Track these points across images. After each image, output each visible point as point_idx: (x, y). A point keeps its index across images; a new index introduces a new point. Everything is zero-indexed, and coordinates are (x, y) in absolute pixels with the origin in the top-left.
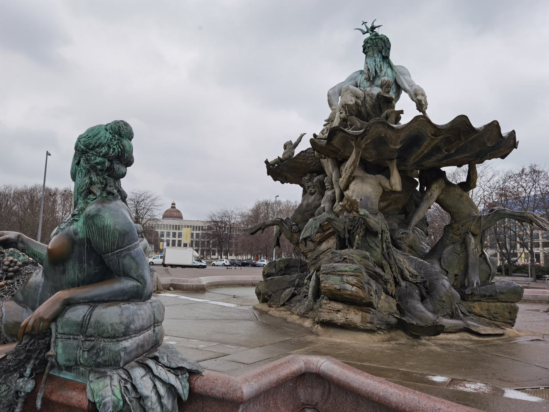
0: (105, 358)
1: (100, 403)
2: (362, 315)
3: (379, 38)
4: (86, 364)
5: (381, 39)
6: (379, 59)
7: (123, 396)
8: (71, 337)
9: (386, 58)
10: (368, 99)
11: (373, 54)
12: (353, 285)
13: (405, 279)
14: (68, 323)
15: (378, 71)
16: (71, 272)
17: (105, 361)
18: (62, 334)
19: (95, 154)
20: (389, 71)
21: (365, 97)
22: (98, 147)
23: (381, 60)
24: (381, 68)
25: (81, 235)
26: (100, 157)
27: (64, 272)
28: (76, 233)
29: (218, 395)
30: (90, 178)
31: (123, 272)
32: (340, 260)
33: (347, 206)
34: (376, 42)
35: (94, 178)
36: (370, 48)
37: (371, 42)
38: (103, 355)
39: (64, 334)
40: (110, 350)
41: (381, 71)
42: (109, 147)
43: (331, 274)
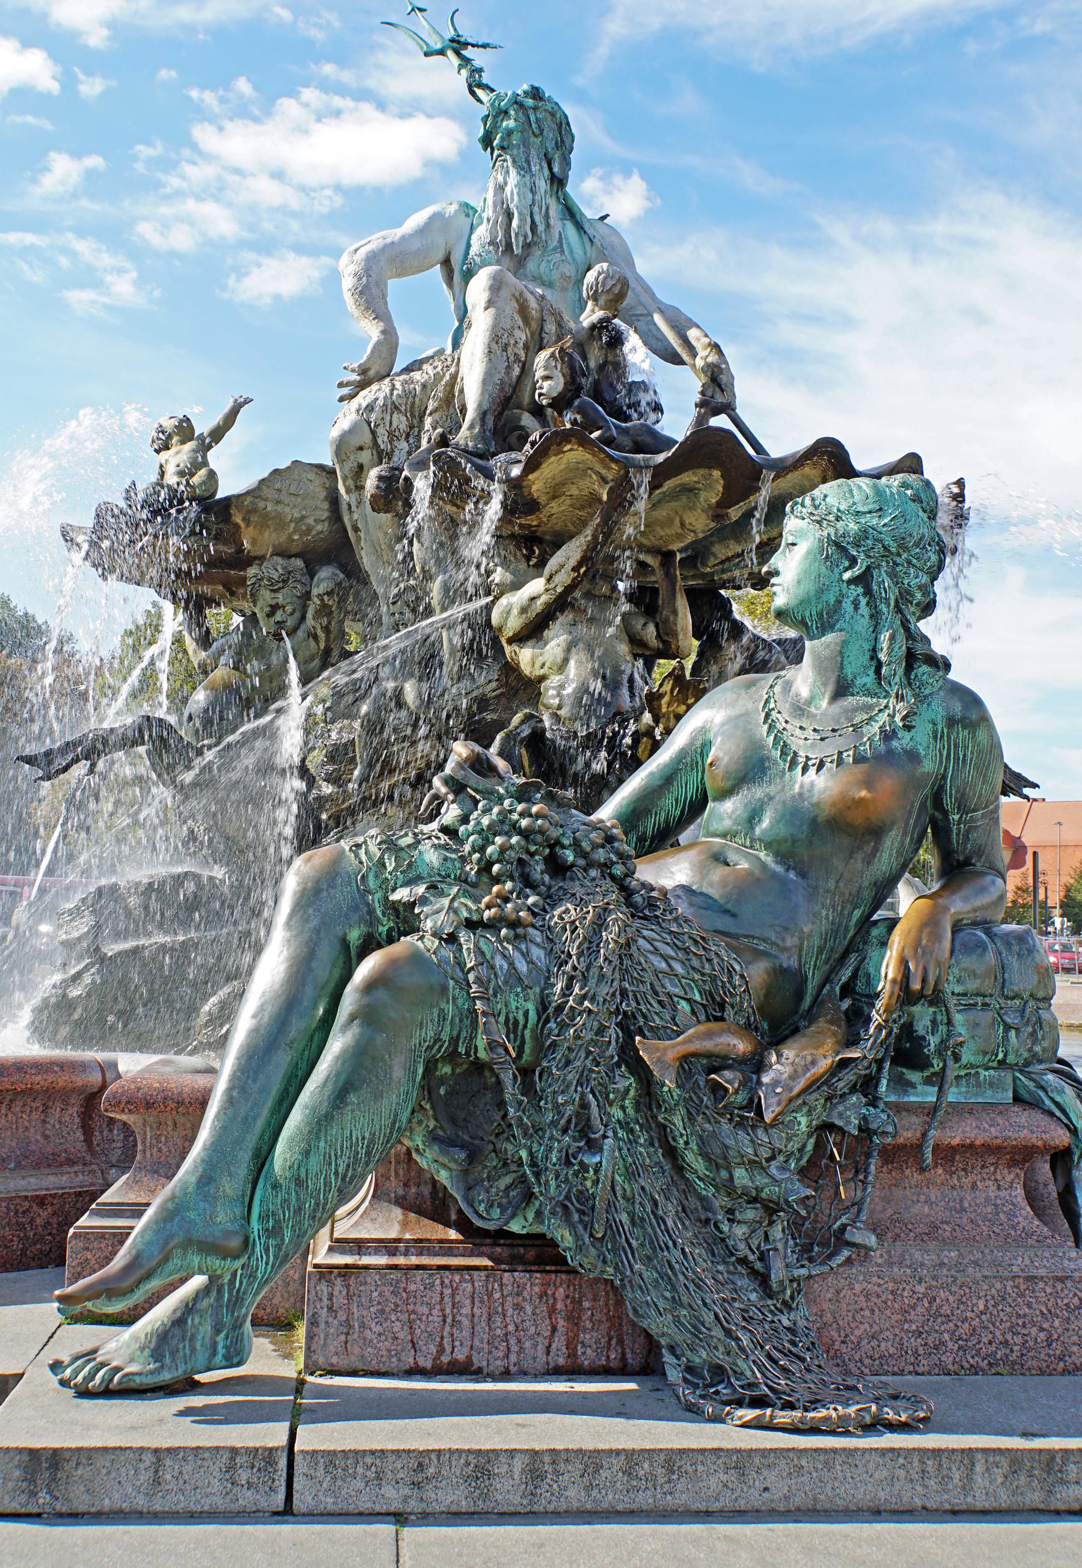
8: (979, 1000)
15: (541, 228)
16: (885, 856)
20: (571, 231)
24: (547, 216)
31: (988, 856)
41: (548, 226)
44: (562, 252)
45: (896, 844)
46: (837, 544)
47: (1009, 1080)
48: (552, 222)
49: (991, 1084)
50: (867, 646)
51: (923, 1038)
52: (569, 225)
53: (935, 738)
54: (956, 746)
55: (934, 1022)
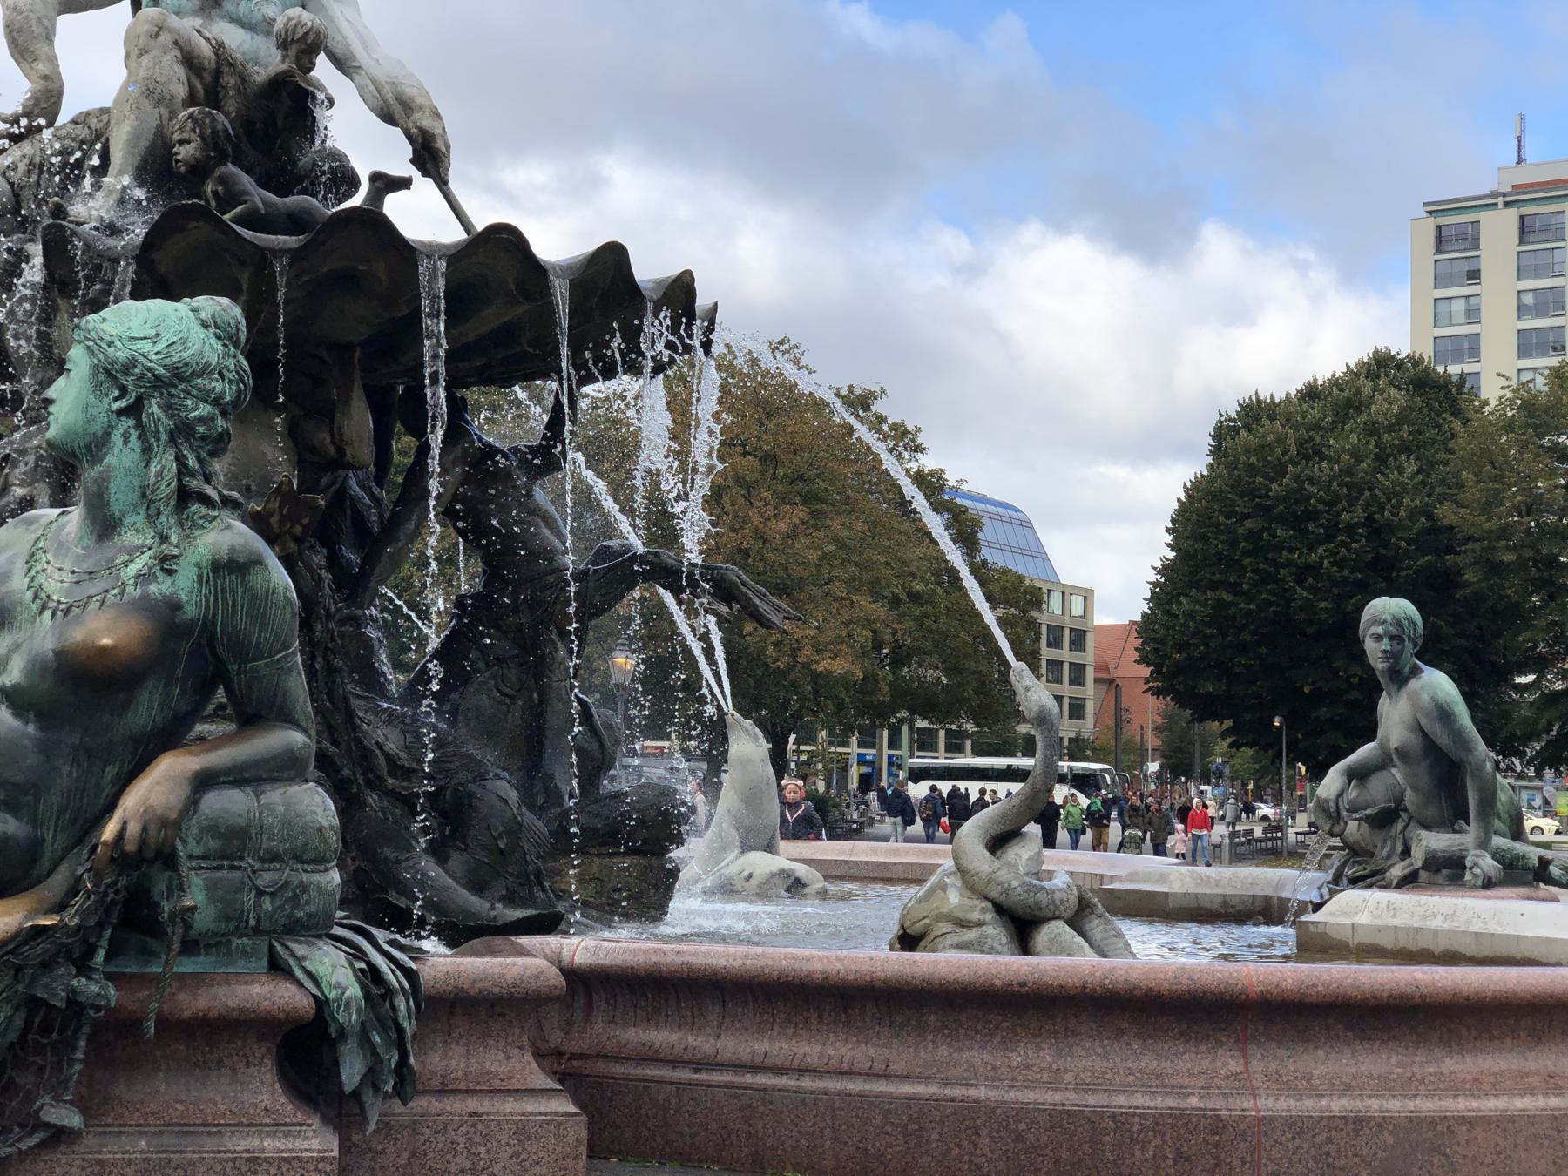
0: (312, 908)
1: (338, 1000)
4: (264, 925)
7: (363, 986)
10: (230, 80)
13: (375, 783)
14: (213, 829)
16: (143, 709)
17: (310, 916)
18: (198, 857)
19: (195, 392)
21: (218, 73)
22: (201, 374)
25: (190, 612)
26: (205, 401)
27: (126, 706)
28: (176, 606)
29: (496, 990)
30: (180, 459)
33: (274, 520)
35: (192, 462)
38: (308, 903)
39: (204, 858)
40: (319, 889)
42: (221, 374)
45: (157, 696)
46: (107, 371)
47: (265, 949)
49: (244, 954)
50: (137, 483)
51: (157, 904)
53: (200, 582)
54: (224, 590)
55: (169, 887)
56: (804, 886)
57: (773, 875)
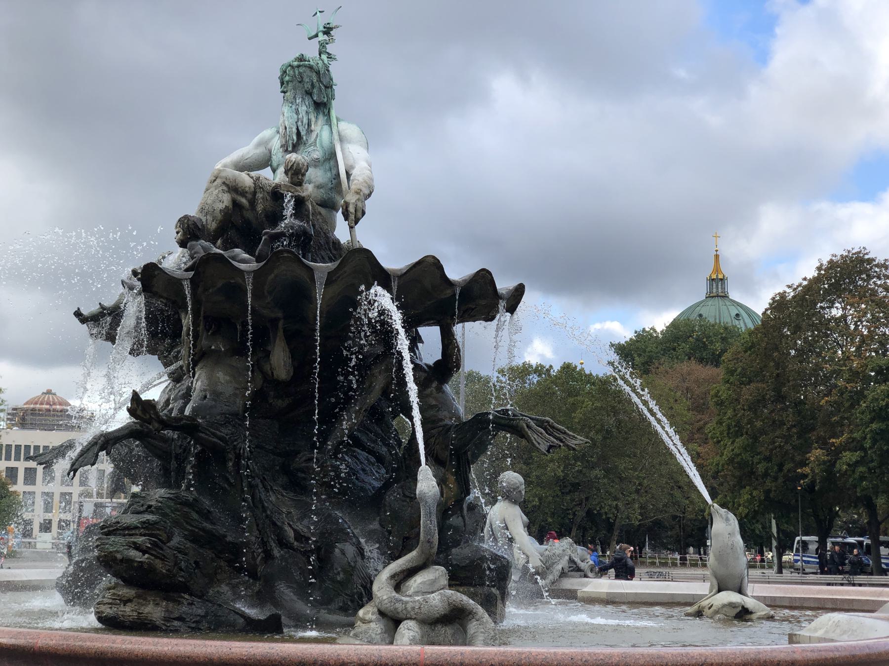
2: (167, 607)
3: (305, 66)
5: (311, 67)
6: (304, 108)
9: (322, 107)
10: (259, 195)
11: (295, 98)
12: (144, 552)
13: (282, 543)
15: (303, 133)
21: (255, 193)
23: (311, 110)
24: (309, 125)
32: (142, 509)
33: (139, 412)
34: (300, 73)
36: (290, 84)
37: (291, 72)
41: (309, 131)
43: (115, 535)
44: (315, 145)
48: (313, 126)
52: (326, 128)
56: (751, 613)
57: (724, 606)
